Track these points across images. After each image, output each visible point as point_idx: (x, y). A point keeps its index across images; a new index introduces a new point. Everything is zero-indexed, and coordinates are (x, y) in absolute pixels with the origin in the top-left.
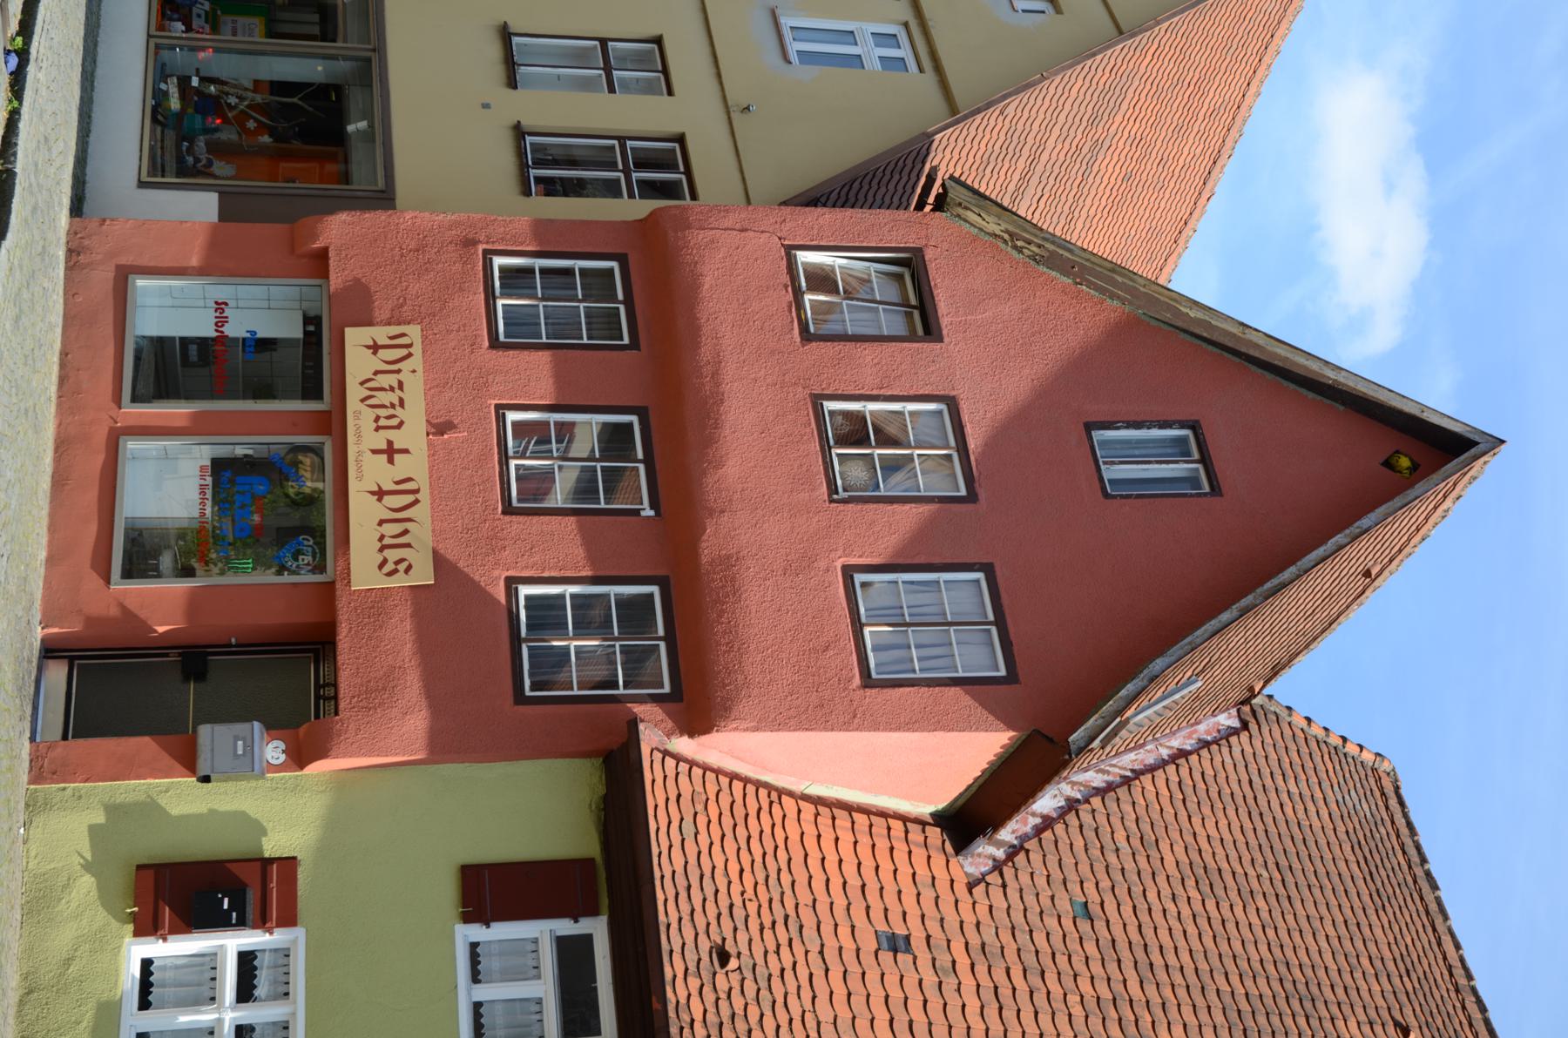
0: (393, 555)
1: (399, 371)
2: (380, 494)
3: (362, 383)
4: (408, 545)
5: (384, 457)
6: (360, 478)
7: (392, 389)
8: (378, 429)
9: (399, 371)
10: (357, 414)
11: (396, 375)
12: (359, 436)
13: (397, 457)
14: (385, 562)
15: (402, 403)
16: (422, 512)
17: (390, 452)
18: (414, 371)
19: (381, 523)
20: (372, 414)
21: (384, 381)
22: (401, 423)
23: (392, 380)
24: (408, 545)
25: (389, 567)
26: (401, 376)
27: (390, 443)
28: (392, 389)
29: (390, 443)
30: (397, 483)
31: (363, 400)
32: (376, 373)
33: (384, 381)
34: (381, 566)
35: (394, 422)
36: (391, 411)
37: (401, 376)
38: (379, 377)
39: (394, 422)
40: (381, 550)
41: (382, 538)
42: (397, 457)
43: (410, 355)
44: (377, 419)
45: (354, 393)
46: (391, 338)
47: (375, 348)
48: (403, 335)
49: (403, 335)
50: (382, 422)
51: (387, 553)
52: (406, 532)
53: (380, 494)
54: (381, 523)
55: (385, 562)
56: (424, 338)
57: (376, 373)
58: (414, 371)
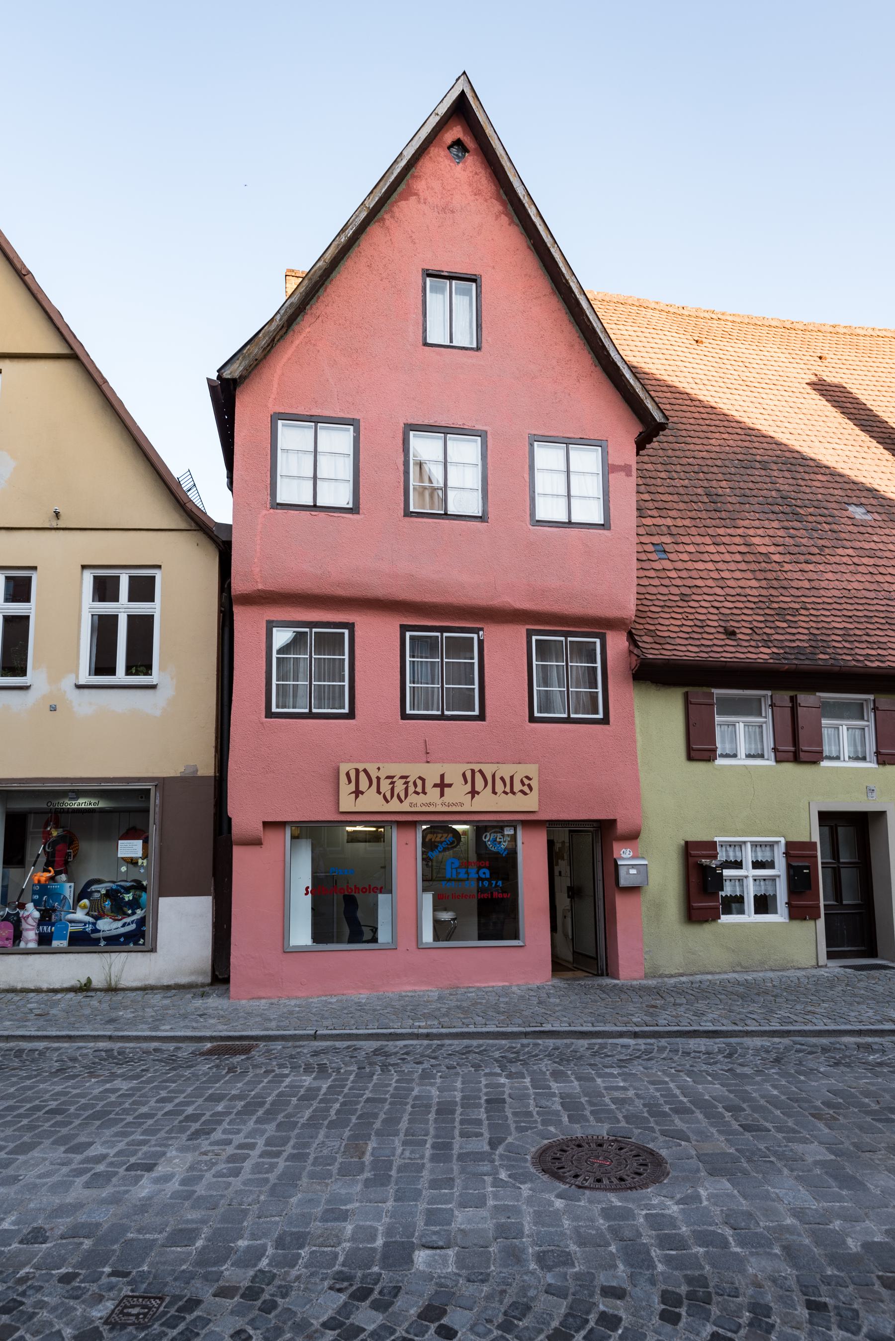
0: (517, 787)
1: (378, 778)
2: (474, 793)
3: (387, 801)
4: (512, 778)
5: (446, 789)
6: (462, 804)
8: (424, 792)
9: (378, 778)
10: (411, 805)
11: (382, 781)
13: (446, 781)
14: (522, 792)
17: (442, 786)
18: (379, 769)
19: (494, 792)
21: (385, 786)
22: (420, 778)
24: (512, 778)
25: (526, 789)
27: (435, 786)
28: (393, 783)
29: (435, 786)
30: (466, 782)
31: (401, 801)
32: (379, 792)
33: (385, 786)
34: (525, 794)
35: (419, 783)
36: (411, 784)
37: (382, 777)
39: (419, 783)
40: (514, 793)
41: (505, 793)
42: (446, 781)
43: (365, 771)
45: (394, 805)
46: (350, 781)
47: (358, 793)
48: (348, 774)
49: (348, 774)
50: (419, 789)
51: (516, 789)
52: (502, 779)
53: (474, 793)
54: (494, 792)
56: (349, 761)
57: (379, 792)
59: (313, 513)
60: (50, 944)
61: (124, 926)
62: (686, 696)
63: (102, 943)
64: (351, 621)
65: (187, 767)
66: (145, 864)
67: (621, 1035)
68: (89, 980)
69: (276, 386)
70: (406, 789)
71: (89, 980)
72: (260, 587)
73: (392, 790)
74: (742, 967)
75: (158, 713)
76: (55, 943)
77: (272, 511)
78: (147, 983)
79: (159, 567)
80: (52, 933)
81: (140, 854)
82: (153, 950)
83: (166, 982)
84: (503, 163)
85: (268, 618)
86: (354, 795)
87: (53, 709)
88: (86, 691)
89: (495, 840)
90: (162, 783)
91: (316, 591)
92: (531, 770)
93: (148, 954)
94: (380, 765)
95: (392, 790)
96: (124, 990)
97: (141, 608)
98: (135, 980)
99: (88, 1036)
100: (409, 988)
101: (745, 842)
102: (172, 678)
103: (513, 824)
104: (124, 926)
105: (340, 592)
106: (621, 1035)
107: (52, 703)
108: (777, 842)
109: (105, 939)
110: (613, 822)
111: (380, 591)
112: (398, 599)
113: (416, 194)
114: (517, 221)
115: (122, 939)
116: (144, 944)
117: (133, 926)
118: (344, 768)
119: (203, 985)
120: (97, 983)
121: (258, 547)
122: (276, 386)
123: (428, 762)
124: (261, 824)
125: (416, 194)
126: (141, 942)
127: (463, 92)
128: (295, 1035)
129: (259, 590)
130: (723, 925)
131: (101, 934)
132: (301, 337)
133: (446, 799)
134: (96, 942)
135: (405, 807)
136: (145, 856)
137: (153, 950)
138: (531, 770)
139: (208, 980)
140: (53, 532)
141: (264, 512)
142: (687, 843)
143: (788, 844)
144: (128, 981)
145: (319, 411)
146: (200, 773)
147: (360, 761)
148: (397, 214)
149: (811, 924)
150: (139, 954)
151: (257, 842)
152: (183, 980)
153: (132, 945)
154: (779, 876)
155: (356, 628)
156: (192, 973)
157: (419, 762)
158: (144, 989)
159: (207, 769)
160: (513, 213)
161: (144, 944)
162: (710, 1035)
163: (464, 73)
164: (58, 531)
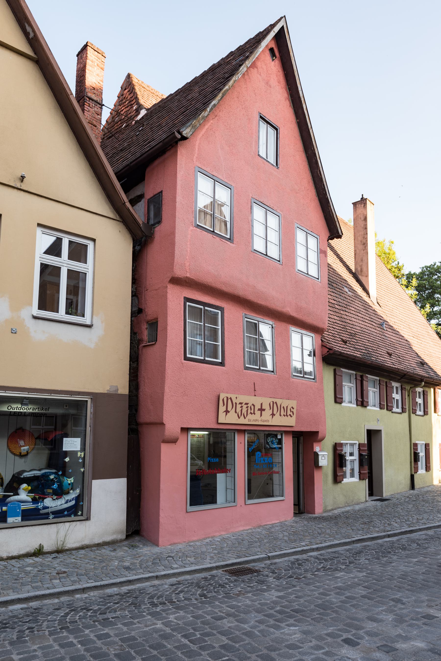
0: (289, 413)
1: (236, 403)
2: (273, 415)
3: (239, 418)
4: (287, 407)
5: (263, 412)
6: (268, 421)
7: (242, 407)
8: (254, 414)
9: (236, 403)
10: (249, 420)
11: (237, 405)
12: (256, 420)
13: (263, 408)
14: (290, 415)
15: (246, 404)
16: (279, 401)
17: (262, 410)
18: (236, 398)
19: (280, 415)
20: (249, 415)
21: (239, 410)
22: (253, 405)
23: (239, 406)
24: (287, 407)
25: (291, 414)
26: (238, 403)
27: (259, 410)
28: (242, 407)
29: (259, 410)
30: (270, 409)
31: (245, 418)
33: (239, 410)
34: (291, 416)
35: (252, 407)
36: (249, 408)
37: (238, 403)
38: (237, 411)
39: (252, 407)
40: (287, 416)
41: (284, 415)
42: (263, 408)
43: (231, 398)
44: (251, 413)
45: (242, 421)
46: (224, 405)
47: (227, 412)
48: (223, 400)
49: (223, 400)
50: (252, 412)
51: (288, 414)
52: (283, 407)
53: (273, 415)
54: (280, 415)
55: (290, 415)
57: (236, 412)
58: (236, 398)
59: (214, 236)
60: (5, 521)
61: (67, 502)
62: (335, 370)
63: (51, 516)
64: (223, 306)
65: (111, 386)
66: (82, 456)
67: (384, 537)
68: (41, 547)
69: (197, 149)
70: (247, 411)
71: (41, 547)
72: (188, 275)
73: (241, 411)
74: (348, 504)
75: (92, 346)
76: (10, 520)
77: (195, 228)
78: (83, 543)
79: (94, 240)
80: (6, 512)
81: (78, 448)
82: (88, 519)
83: (97, 540)
84: (295, 74)
85: (185, 296)
86: (225, 413)
87: (13, 332)
88: (41, 322)
89: (272, 441)
90: (95, 396)
91: (214, 285)
92: (292, 403)
93: (84, 522)
94: (237, 396)
95: (241, 411)
96: (67, 550)
97: (77, 266)
98: (75, 542)
99: (142, 578)
100: (241, 529)
101: (347, 444)
102: (102, 322)
103: (282, 433)
104: (67, 502)
105: (224, 288)
106: (384, 537)
107: (14, 328)
108: (355, 444)
109: (53, 513)
110: (317, 432)
111: (241, 292)
112: (247, 299)
113: (257, 68)
114: (292, 106)
115: (66, 513)
116: (82, 515)
117: (73, 502)
118: (222, 396)
119: (121, 541)
120: (46, 548)
121: (188, 249)
122: (197, 149)
123: (255, 396)
124: (180, 430)
125: (257, 68)
126: (80, 513)
127: (283, 27)
128: (259, 558)
129: (187, 277)
130: (347, 483)
131: (50, 510)
132: (209, 124)
133: (263, 418)
134: (46, 516)
135: (246, 422)
136: (83, 449)
137: (88, 519)
138: (292, 403)
139: (124, 537)
140: (16, 190)
141: (191, 228)
142: (336, 443)
143: (359, 444)
144: (71, 543)
145: (217, 174)
146: (120, 392)
147: (227, 393)
148: (249, 74)
149: (364, 481)
150: (78, 523)
151: (174, 441)
152: (108, 538)
153: (73, 516)
154: (355, 460)
155: (225, 311)
156: (114, 533)
157: (252, 396)
158: (82, 548)
159: (124, 389)
160: (291, 101)
161: (82, 515)
162: (410, 532)
163: (285, 16)
164: (19, 191)
